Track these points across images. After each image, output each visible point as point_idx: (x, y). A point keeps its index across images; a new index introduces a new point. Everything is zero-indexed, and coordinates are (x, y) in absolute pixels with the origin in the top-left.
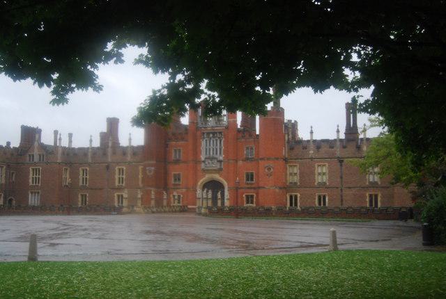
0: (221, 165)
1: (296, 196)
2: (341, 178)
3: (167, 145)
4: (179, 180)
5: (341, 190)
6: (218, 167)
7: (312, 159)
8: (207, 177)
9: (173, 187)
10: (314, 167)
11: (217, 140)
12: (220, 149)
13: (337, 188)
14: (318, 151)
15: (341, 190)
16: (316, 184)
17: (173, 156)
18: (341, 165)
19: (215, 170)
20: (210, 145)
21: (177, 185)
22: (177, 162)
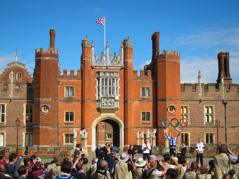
0: (117, 105)
1: (186, 135)
2: (225, 118)
4: (72, 119)
5: (226, 129)
6: (116, 106)
7: (200, 101)
8: (104, 116)
9: (64, 125)
10: (203, 108)
11: (113, 79)
12: (117, 88)
13: (223, 127)
14: (206, 94)
15: (226, 129)
16: (204, 123)
18: (225, 107)
19: (112, 109)
20: (106, 84)
21: (69, 124)
22: (69, 100)
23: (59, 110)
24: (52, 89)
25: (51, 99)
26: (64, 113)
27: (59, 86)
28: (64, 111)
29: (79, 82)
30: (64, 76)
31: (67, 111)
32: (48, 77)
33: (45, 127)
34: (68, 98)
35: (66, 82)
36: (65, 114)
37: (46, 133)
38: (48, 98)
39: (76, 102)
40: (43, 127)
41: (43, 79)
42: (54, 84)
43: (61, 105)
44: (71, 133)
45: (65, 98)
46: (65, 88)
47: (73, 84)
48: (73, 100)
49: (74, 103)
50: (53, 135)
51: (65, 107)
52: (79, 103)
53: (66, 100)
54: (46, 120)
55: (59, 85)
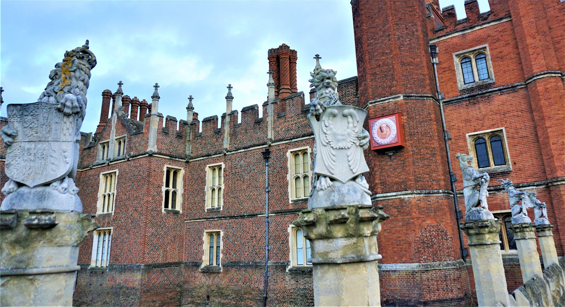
3: (433, 47)
17: (459, 77)
22: (477, 94)
23: (452, 134)
24: (403, 64)
25: (402, 98)
26: (465, 141)
27: (436, 60)
28: (467, 135)
29: (500, 29)
30: (446, 27)
31: (475, 131)
32: (384, 32)
33: (394, 194)
34: (472, 89)
35: (455, 40)
36: (470, 143)
37: (400, 217)
38: (391, 95)
39: (504, 97)
40: (389, 194)
41: (372, 41)
42: (410, 48)
43: (452, 117)
44: (505, 209)
45: (463, 91)
46: (456, 60)
47: (480, 41)
48: (490, 90)
49: (498, 100)
50: (428, 222)
51: (467, 121)
52: (516, 94)
53: (467, 95)
54: (395, 169)
55: (433, 55)
